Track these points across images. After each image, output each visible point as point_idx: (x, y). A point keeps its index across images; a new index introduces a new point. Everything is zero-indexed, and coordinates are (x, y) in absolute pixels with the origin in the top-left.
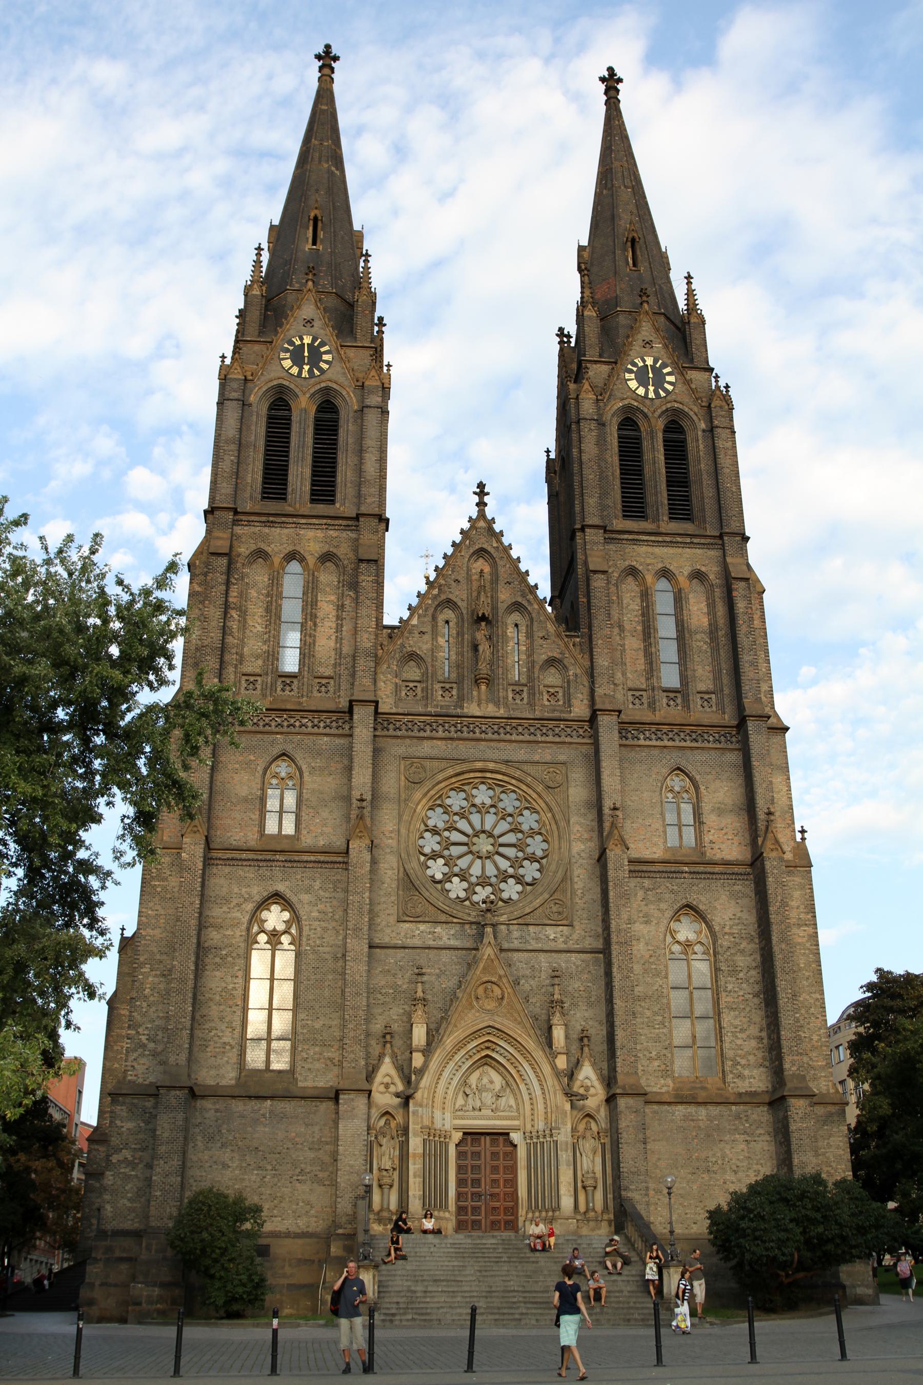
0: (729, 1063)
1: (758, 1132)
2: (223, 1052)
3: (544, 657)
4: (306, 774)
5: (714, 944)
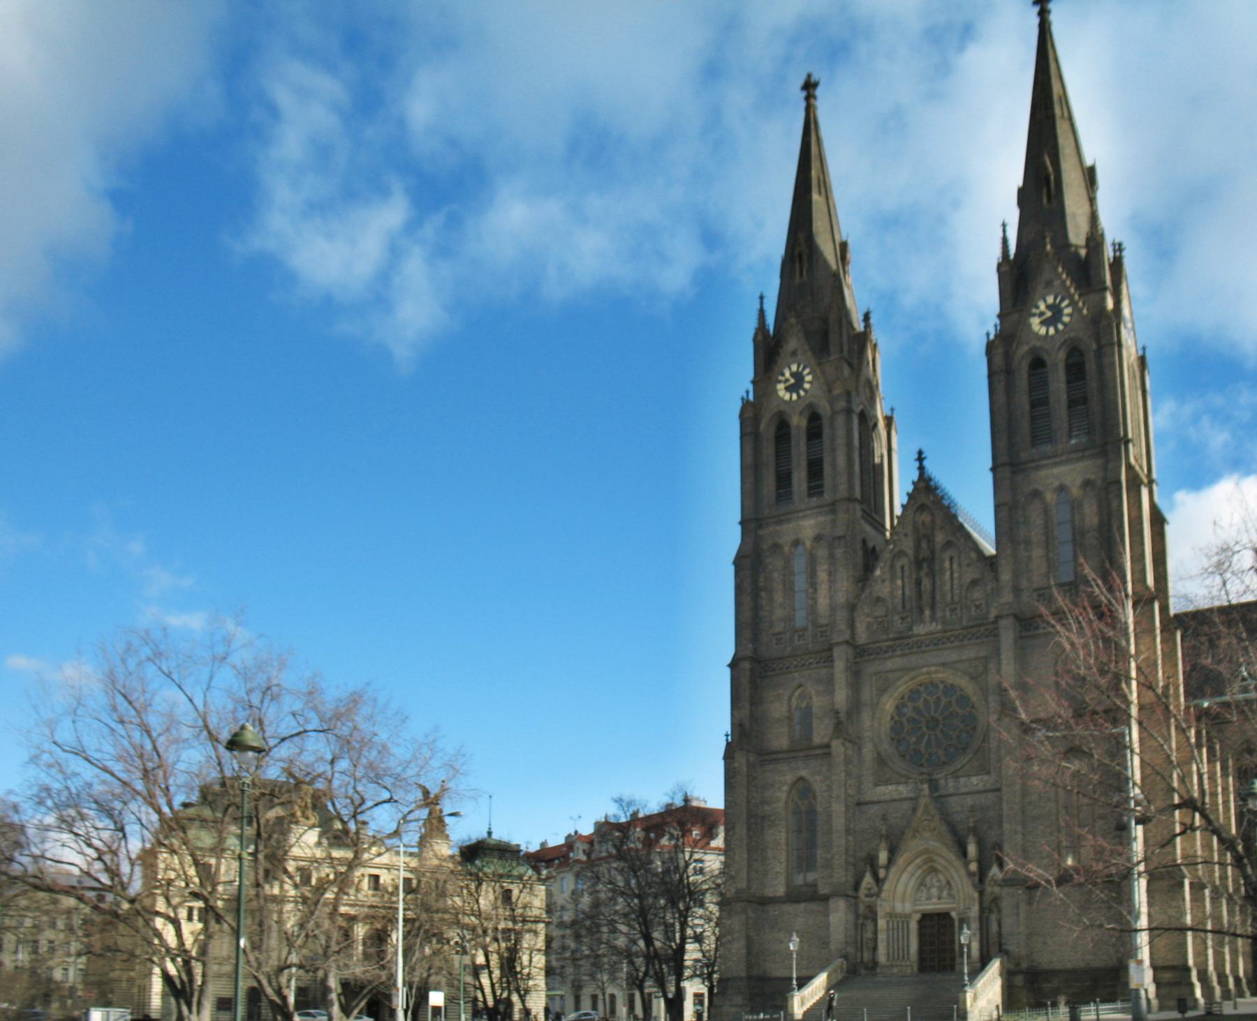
3: (969, 580)
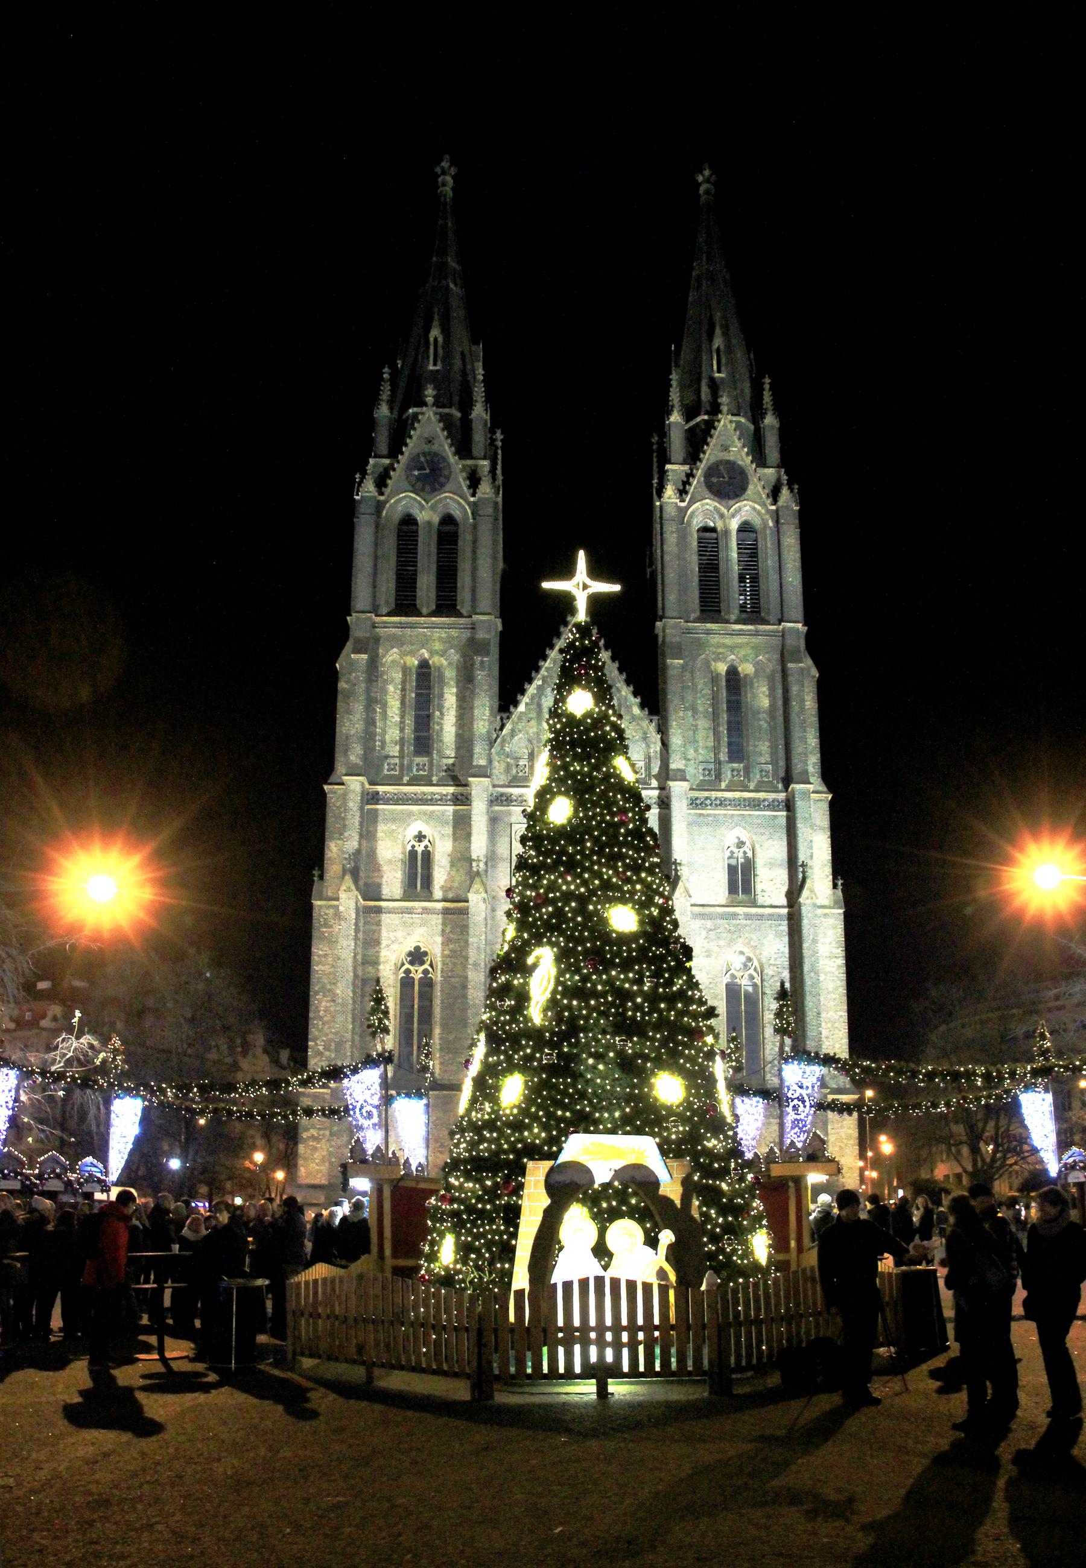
4: (437, 841)
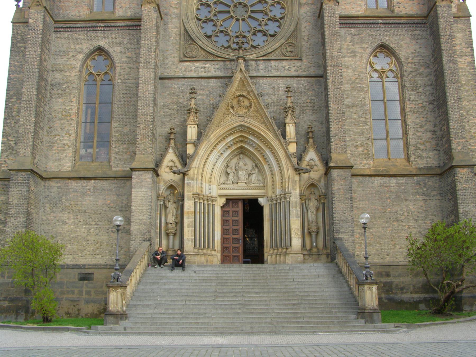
0: (412, 148)
1: (432, 194)
2: (64, 150)
5: (401, 70)
